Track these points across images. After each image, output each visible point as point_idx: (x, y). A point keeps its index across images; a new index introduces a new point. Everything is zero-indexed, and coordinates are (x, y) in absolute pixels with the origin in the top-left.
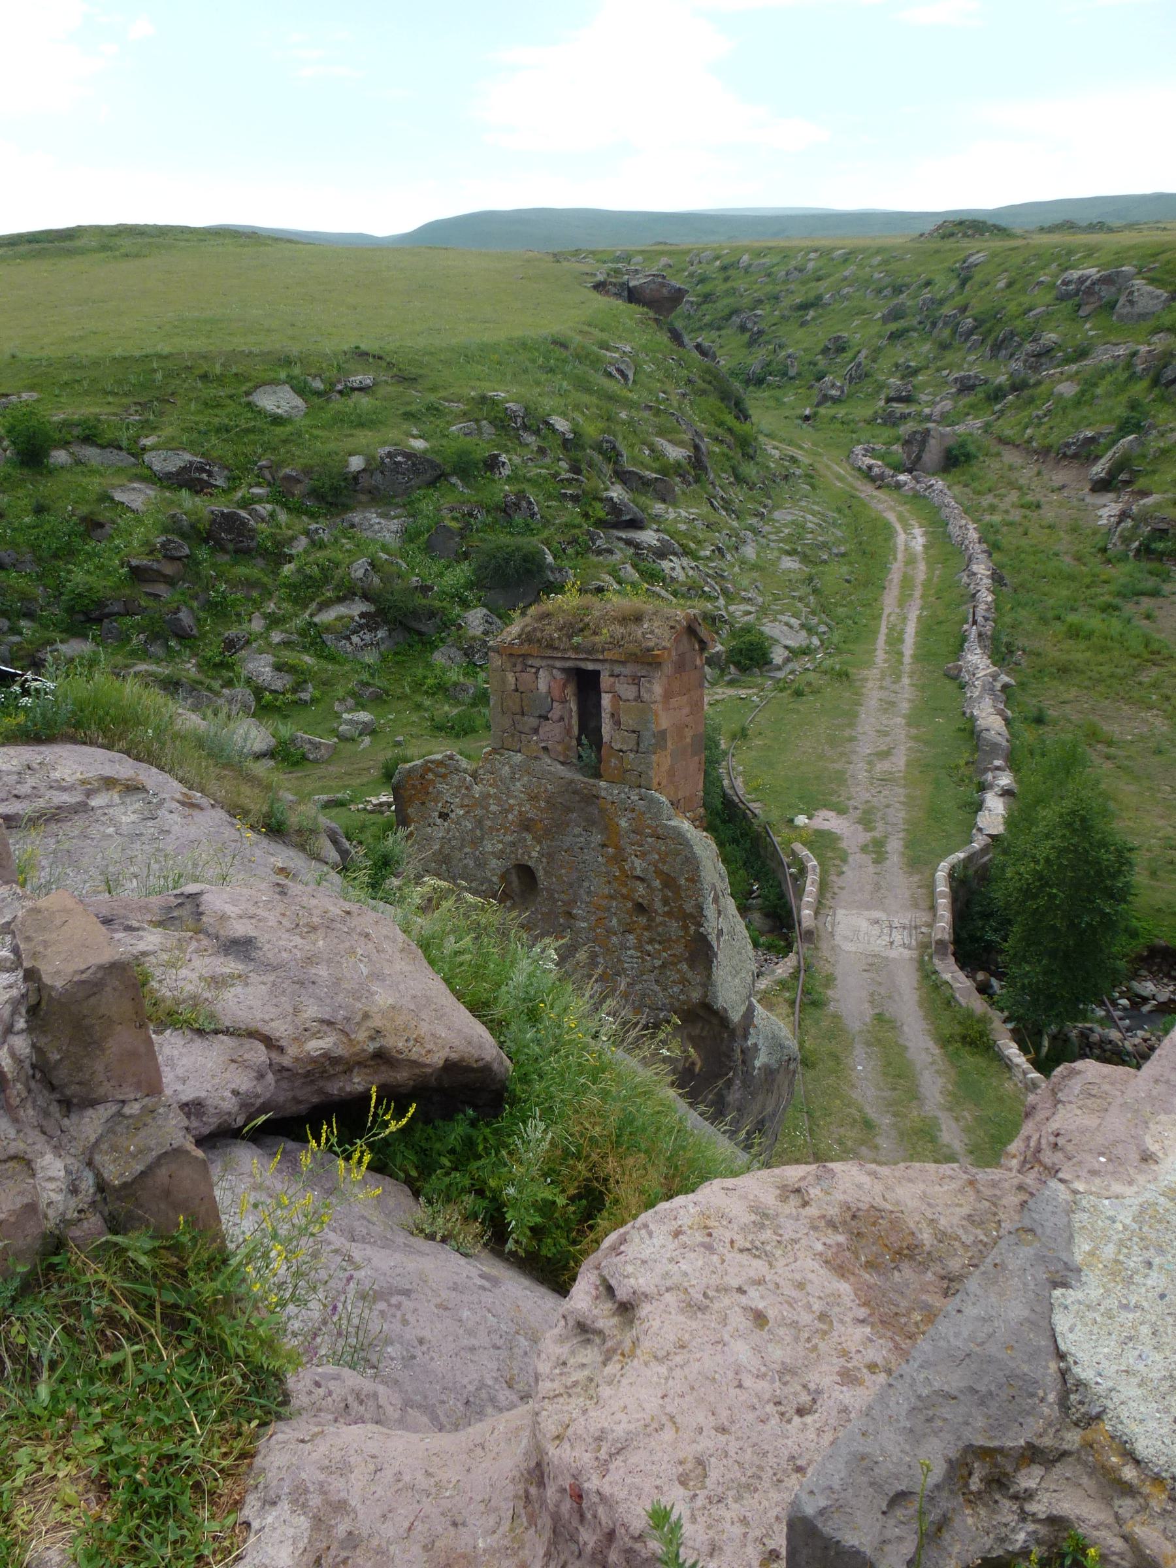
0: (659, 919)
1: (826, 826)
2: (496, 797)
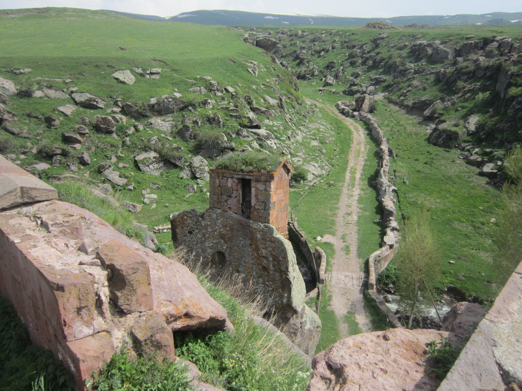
0: (271, 272)
1: (328, 241)
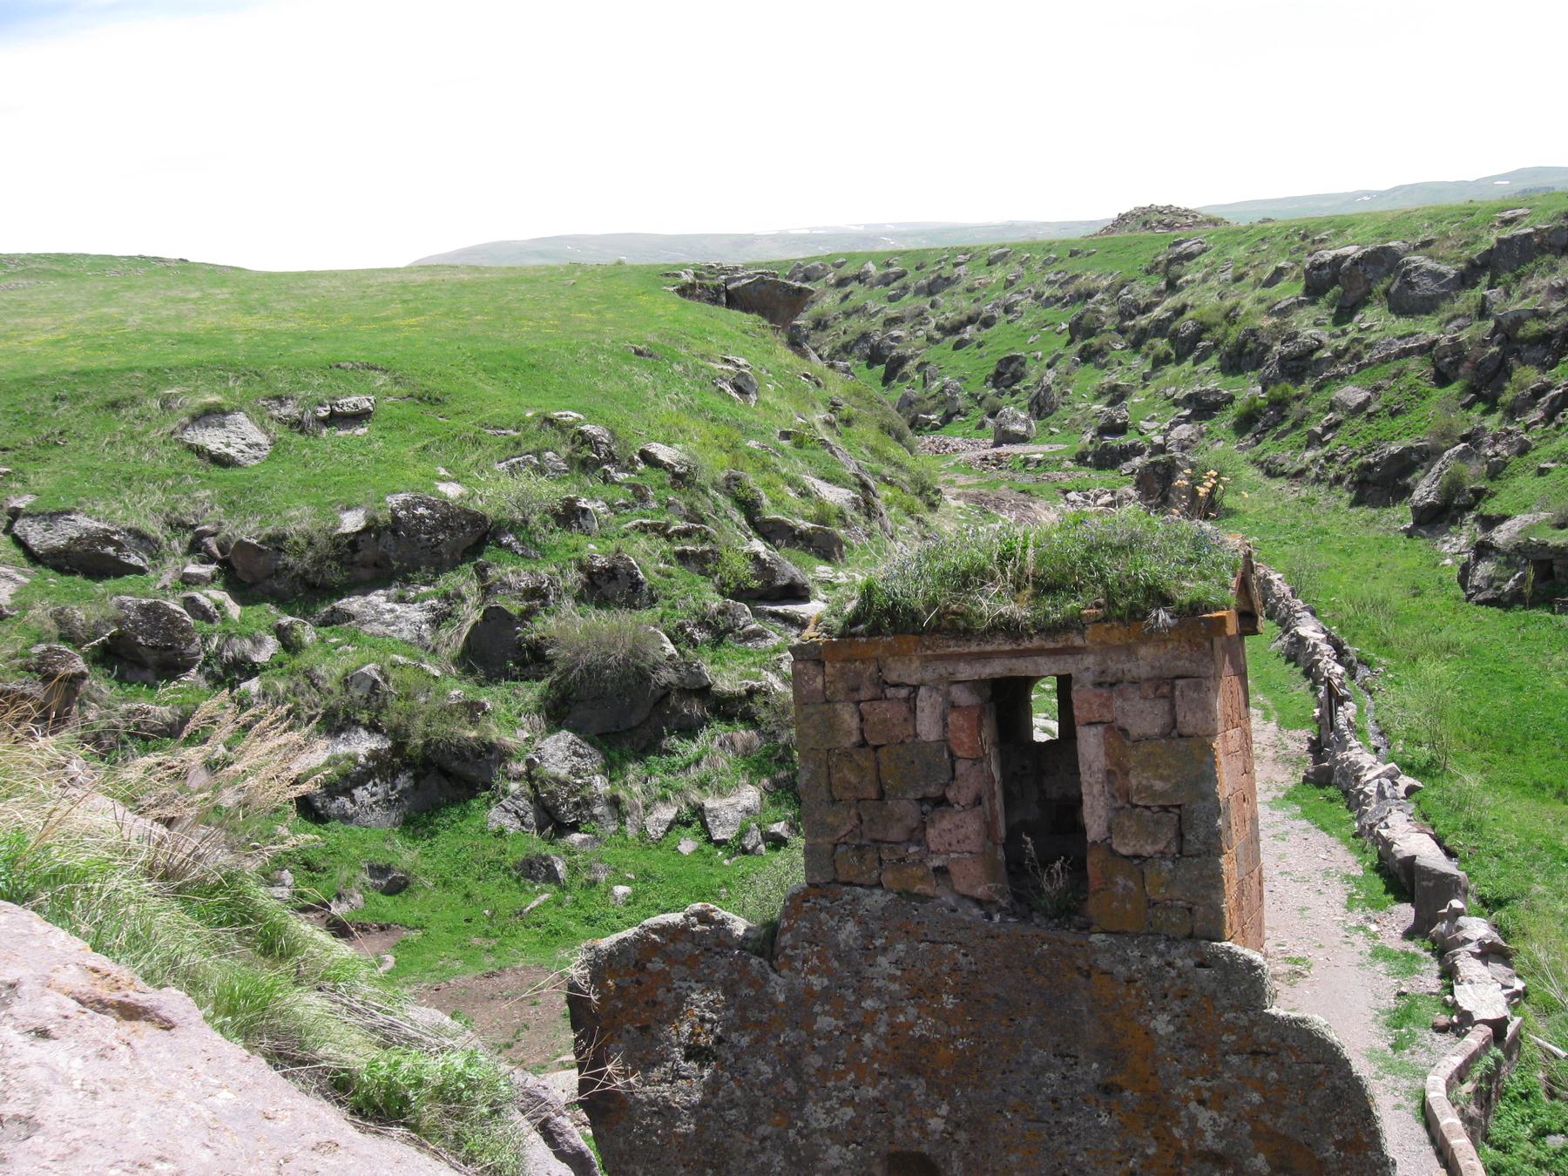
2: (826, 995)
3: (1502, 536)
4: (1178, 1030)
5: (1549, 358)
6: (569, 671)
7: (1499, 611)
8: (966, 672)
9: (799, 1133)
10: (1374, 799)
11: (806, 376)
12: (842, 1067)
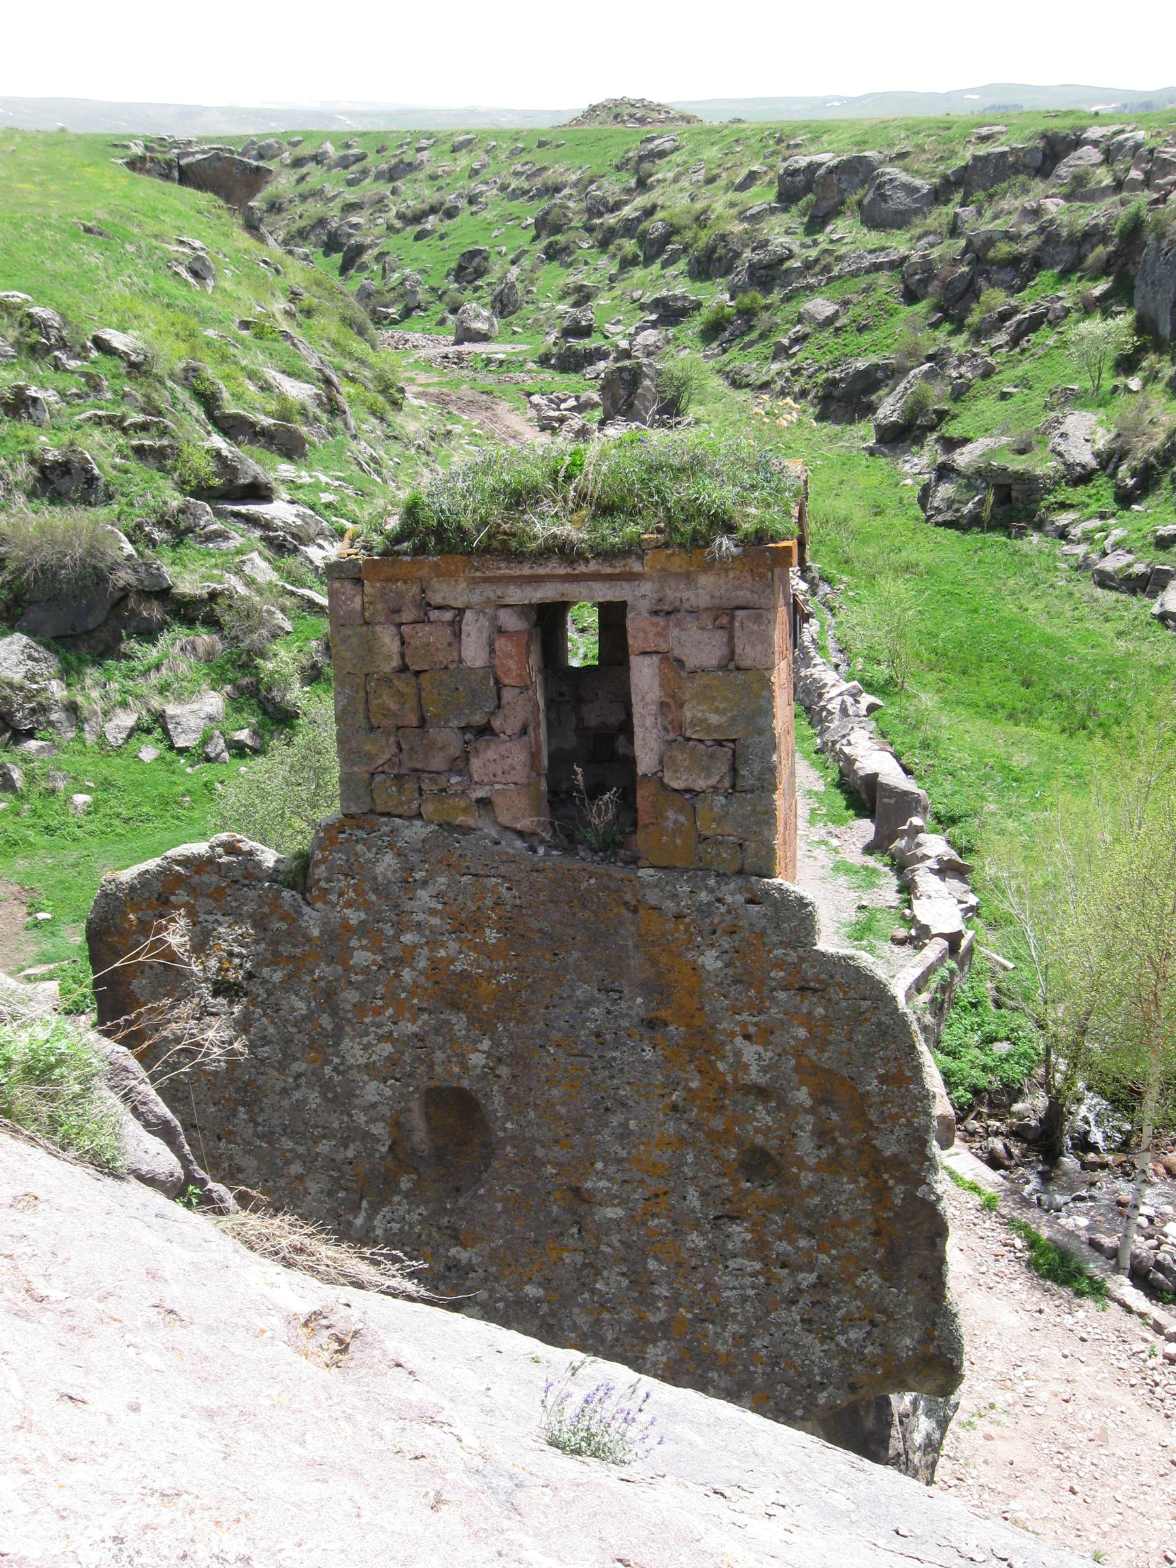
2: (363, 930)
3: (963, 458)
4: (727, 966)
5: (1017, 281)
6: (22, 570)
7: (957, 533)
8: (516, 595)
9: (335, 1069)
10: (837, 716)
11: (265, 262)
12: (380, 1003)
